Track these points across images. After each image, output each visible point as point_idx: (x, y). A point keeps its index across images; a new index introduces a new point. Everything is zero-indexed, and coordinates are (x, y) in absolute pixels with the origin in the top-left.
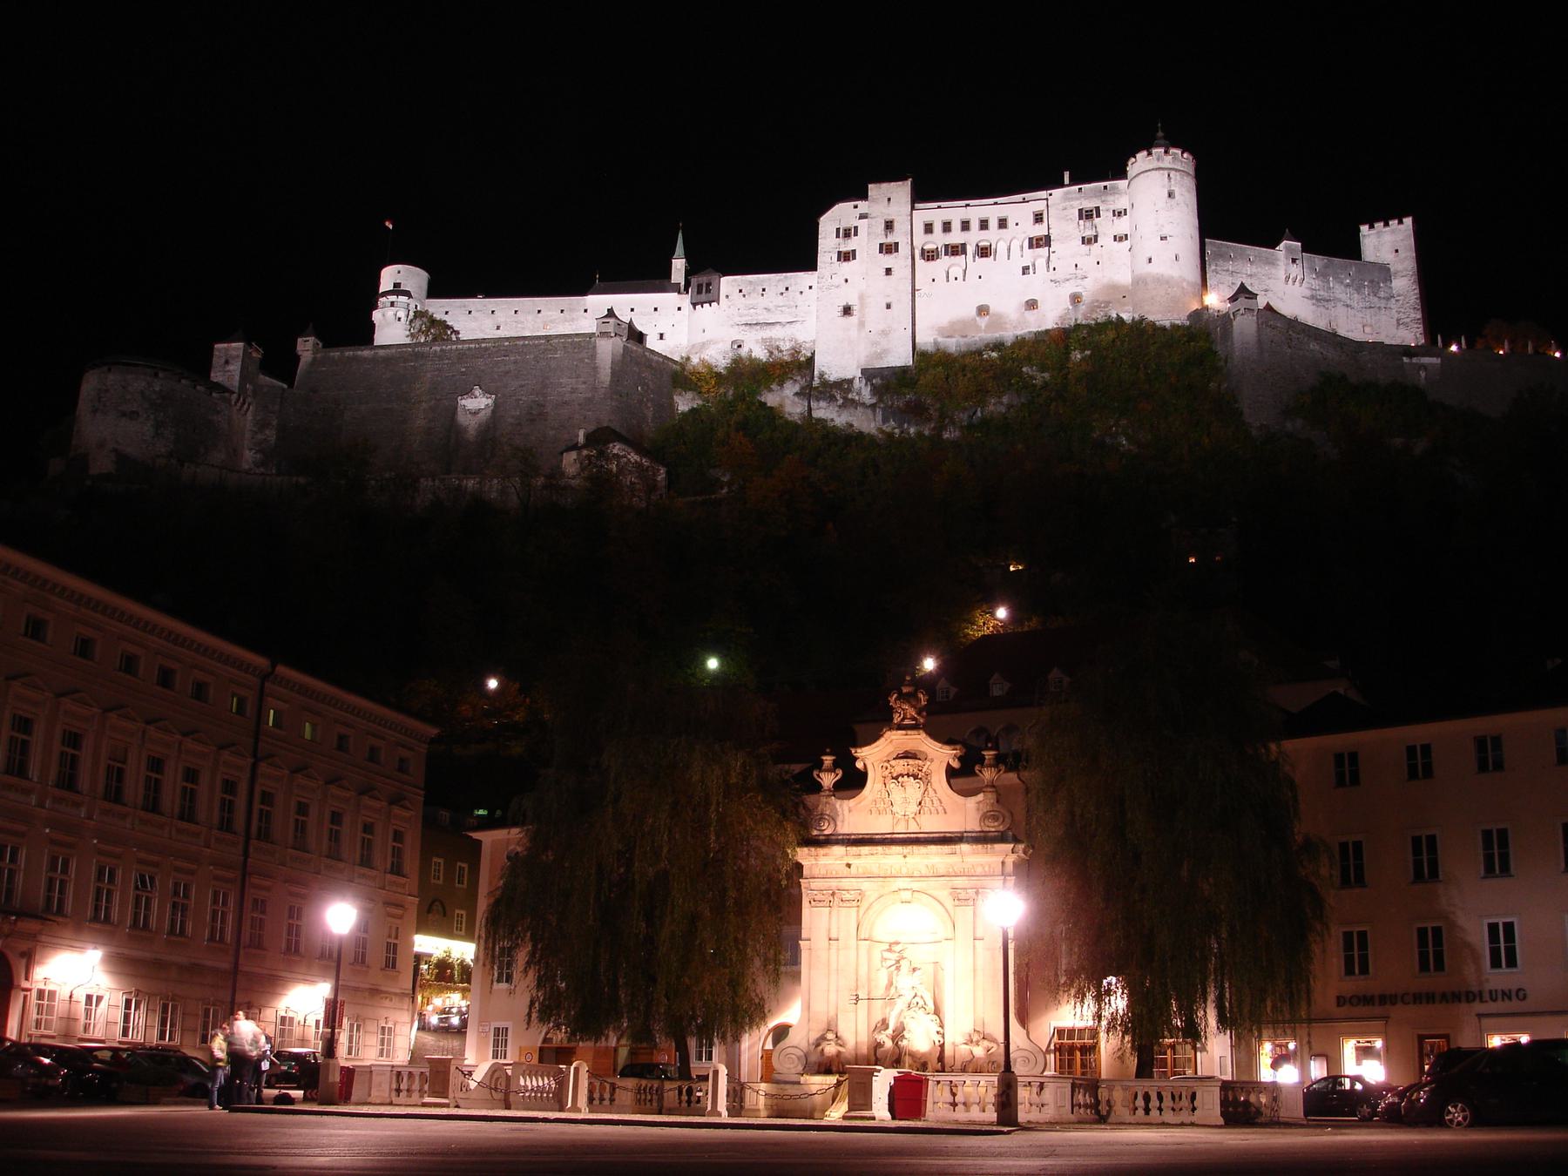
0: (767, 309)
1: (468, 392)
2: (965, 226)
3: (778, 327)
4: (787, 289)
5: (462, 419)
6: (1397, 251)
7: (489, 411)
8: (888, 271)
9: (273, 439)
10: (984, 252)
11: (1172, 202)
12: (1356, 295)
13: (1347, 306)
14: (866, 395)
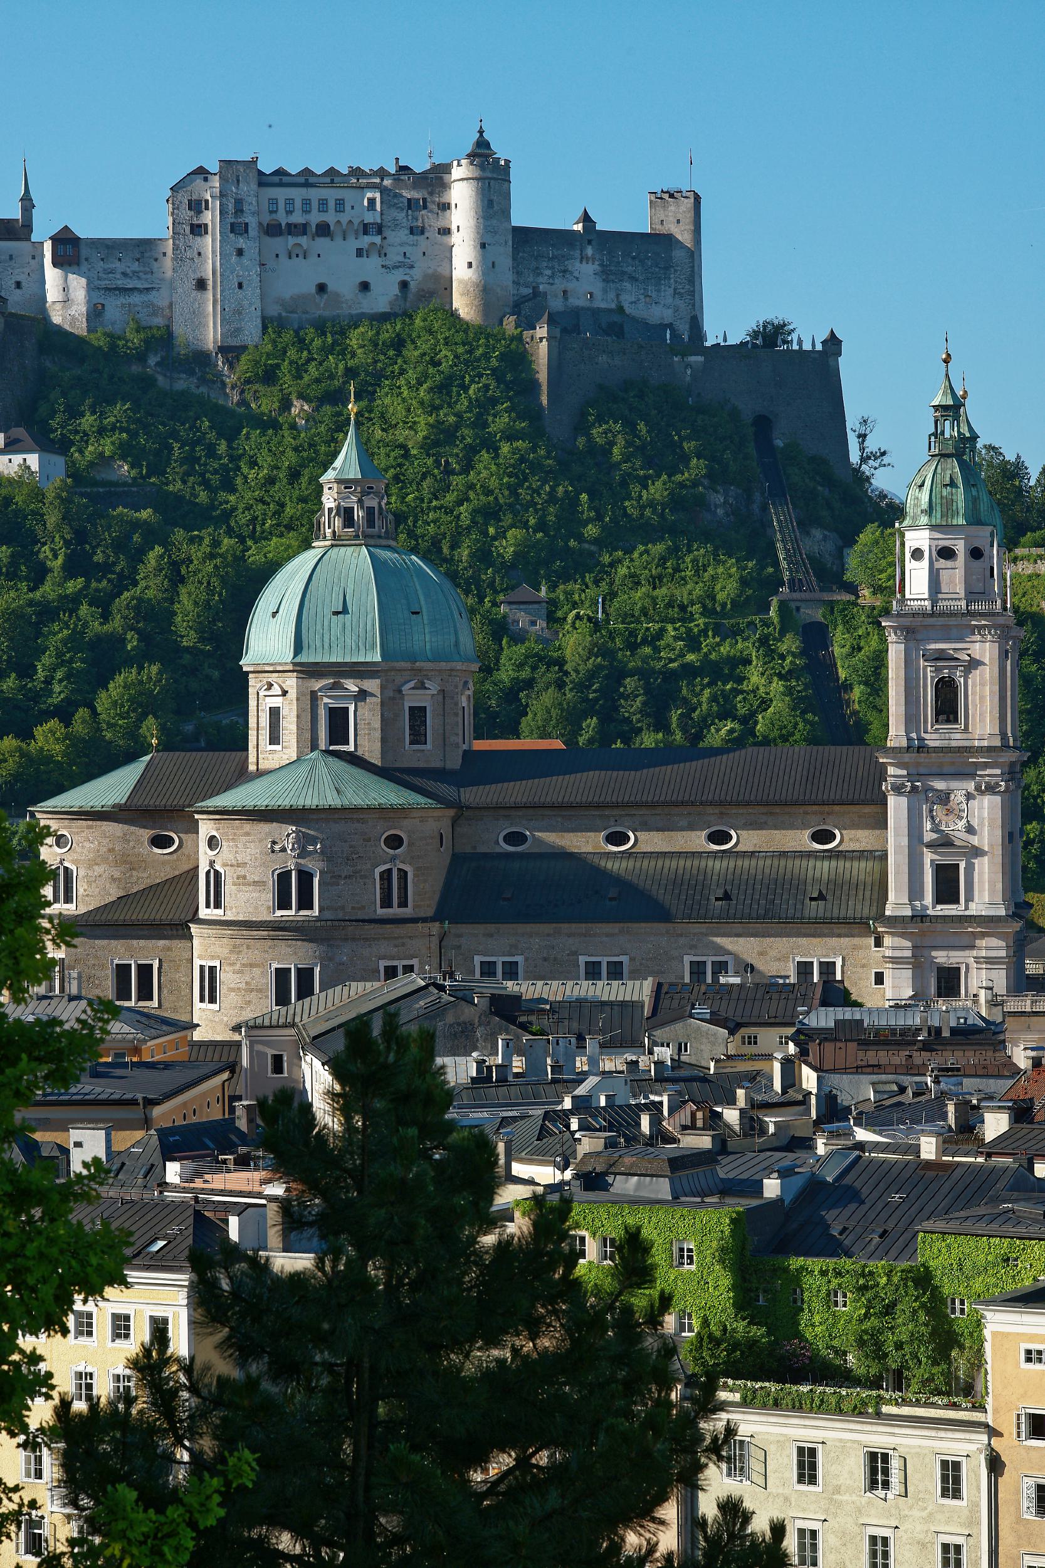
0: (124, 274)
2: (307, 203)
6: (678, 222)
8: (240, 252)
10: (324, 230)
13: (633, 279)
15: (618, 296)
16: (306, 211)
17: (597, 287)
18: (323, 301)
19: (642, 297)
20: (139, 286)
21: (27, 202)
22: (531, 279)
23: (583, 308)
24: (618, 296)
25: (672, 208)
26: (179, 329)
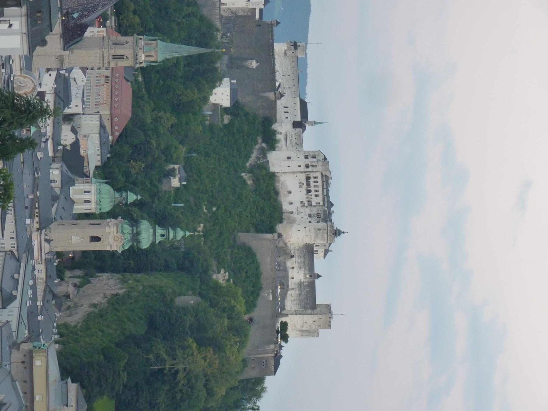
0: (291, 140)
1: (257, 62)
2: (317, 186)
3: (285, 143)
4: (298, 145)
5: (249, 61)
6: (321, 311)
7: (252, 67)
8: (300, 166)
9: (240, 14)
10: (309, 191)
11: (317, 230)
12: (304, 297)
13: (300, 294)
14: (262, 161)
15: (293, 289)
16: (315, 186)
17: (296, 280)
18: (286, 193)
19: (294, 298)
20: (288, 143)
21: (315, 123)
22: (297, 254)
23: (288, 275)
24: (293, 289)
25: (325, 309)
26: (274, 152)
